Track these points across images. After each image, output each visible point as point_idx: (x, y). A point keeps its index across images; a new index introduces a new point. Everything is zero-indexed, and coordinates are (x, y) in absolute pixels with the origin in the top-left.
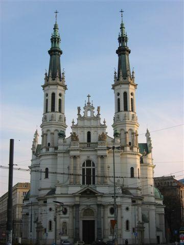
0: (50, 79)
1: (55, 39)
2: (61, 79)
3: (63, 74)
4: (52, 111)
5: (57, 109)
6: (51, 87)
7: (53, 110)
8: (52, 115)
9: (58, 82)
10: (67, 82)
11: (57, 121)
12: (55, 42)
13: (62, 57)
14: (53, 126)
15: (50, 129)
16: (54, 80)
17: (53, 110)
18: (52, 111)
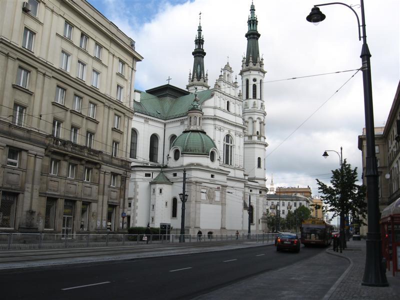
0: (251, 65)
1: (253, 21)
2: (261, 64)
3: (262, 59)
4: (253, 98)
5: (258, 96)
6: (252, 72)
7: (255, 96)
8: (254, 102)
9: (259, 67)
10: (265, 68)
11: (250, 108)
12: (253, 25)
13: (260, 40)
14: (256, 113)
15: (253, 116)
16: (255, 65)
17: (255, 96)
18: (253, 98)
